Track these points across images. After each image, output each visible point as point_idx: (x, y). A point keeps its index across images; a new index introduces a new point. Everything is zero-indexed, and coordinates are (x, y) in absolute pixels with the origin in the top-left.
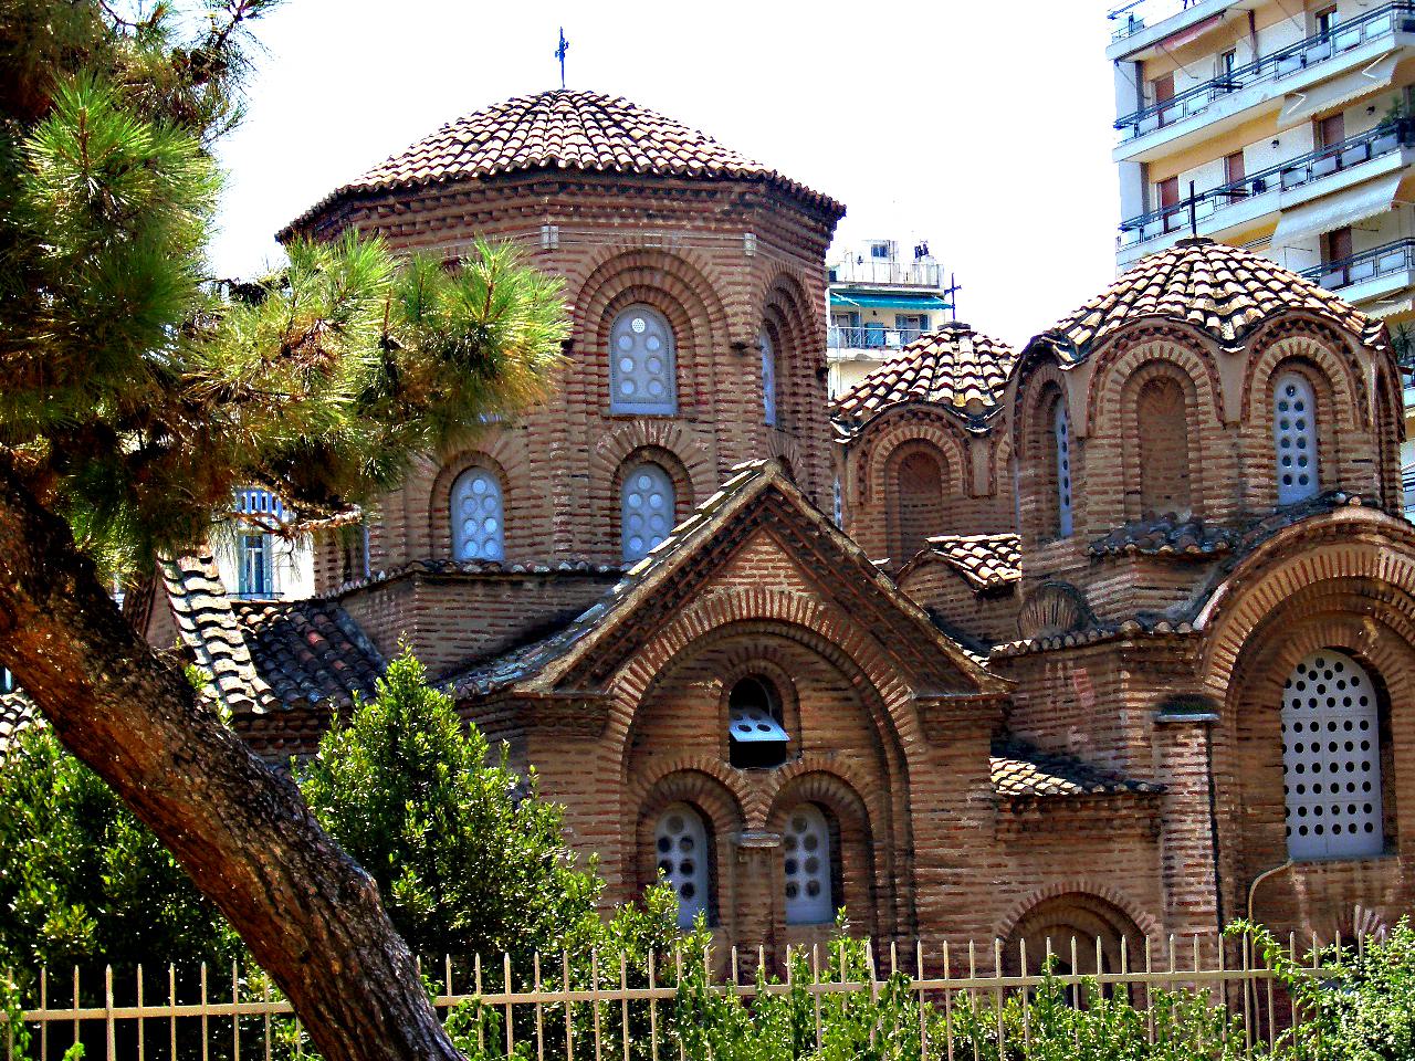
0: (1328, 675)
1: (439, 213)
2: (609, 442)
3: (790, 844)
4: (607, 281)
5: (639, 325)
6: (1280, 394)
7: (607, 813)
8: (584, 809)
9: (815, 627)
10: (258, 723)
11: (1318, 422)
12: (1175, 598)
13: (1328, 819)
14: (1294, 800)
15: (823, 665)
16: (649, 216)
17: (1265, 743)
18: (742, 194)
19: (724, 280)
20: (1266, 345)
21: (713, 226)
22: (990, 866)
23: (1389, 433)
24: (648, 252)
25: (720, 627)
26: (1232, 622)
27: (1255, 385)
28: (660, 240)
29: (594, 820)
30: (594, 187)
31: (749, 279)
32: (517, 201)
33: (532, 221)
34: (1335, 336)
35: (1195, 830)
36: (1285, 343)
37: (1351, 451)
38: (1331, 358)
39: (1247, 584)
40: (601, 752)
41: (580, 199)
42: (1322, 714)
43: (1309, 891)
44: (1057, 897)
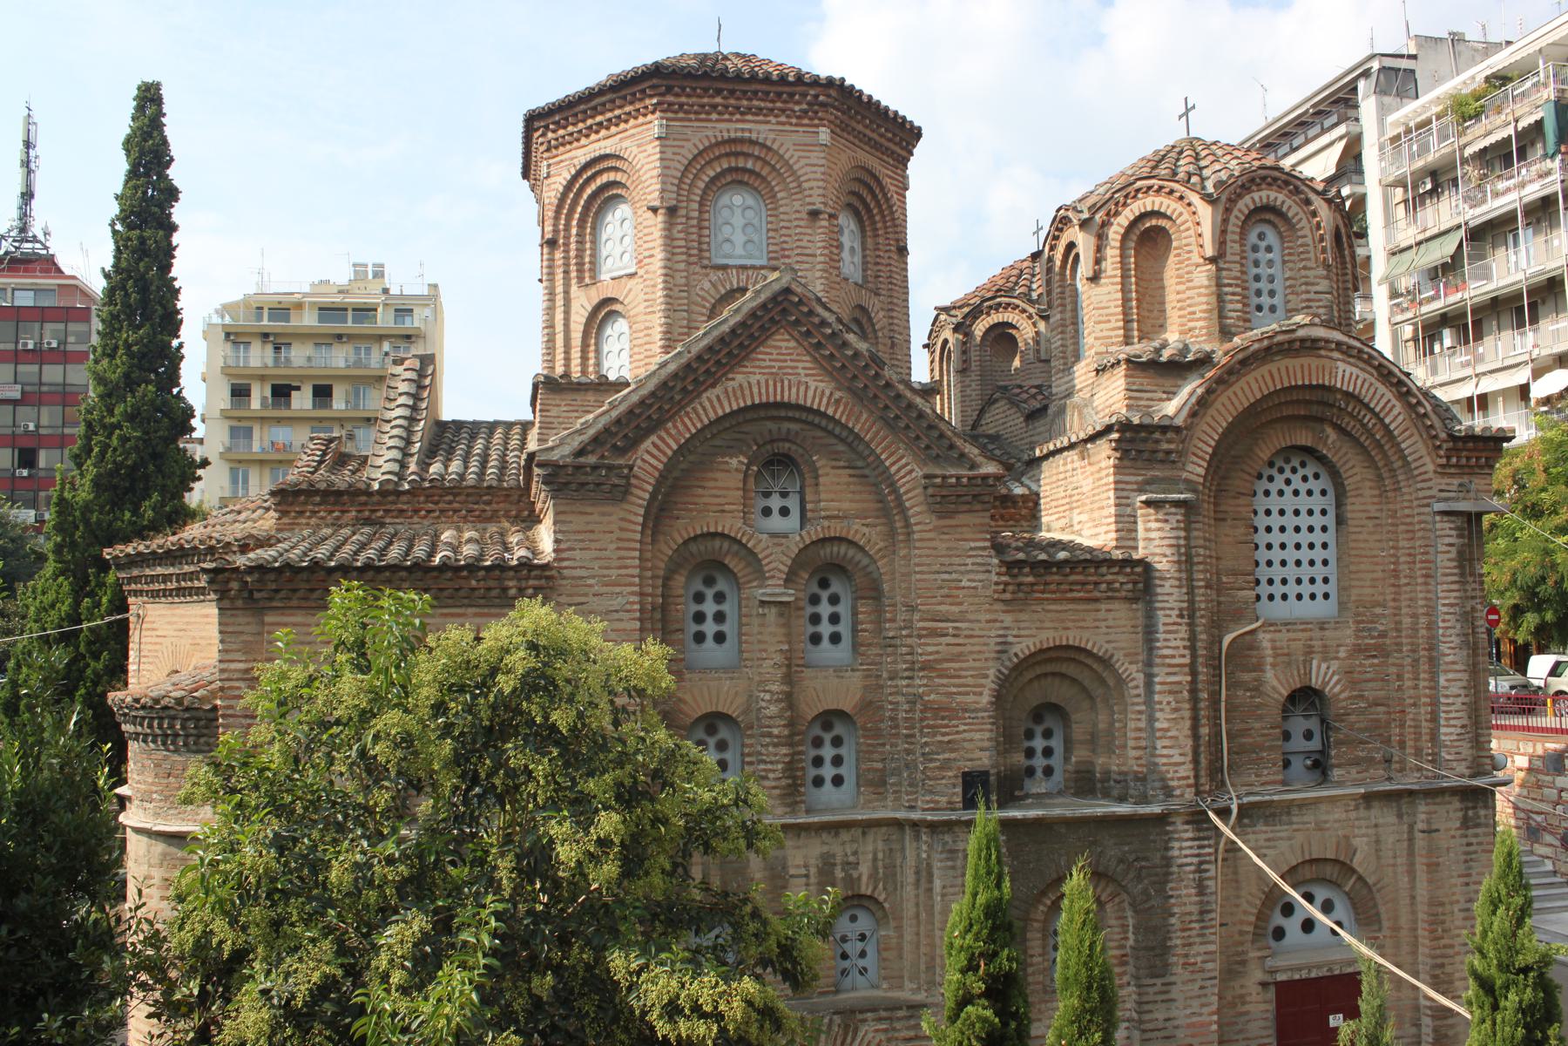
0: (1294, 471)
2: (707, 285)
3: (815, 600)
4: (707, 163)
5: (737, 200)
6: (1253, 237)
7: (626, 567)
8: (602, 563)
9: (830, 412)
10: (404, 498)
12: (1161, 400)
13: (1292, 589)
14: (1263, 573)
15: (841, 447)
16: (742, 114)
18: (816, 96)
19: (803, 162)
20: (1240, 196)
21: (794, 121)
22: (988, 621)
23: (1345, 282)
24: (741, 141)
25: (733, 413)
26: (1209, 419)
27: (1230, 228)
28: (750, 131)
29: (614, 572)
30: (694, 89)
31: (823, 162)
34: (1297, 191)
35: (1169, 596)
36: (1256, 196)
37: (1313, 284)
38: (1295, 209)
39: (1221, 388)
40: (622, 514)
41: (683, 99)
42: (1288, 502)
43: (1274, 648)
44: (1049, 649)
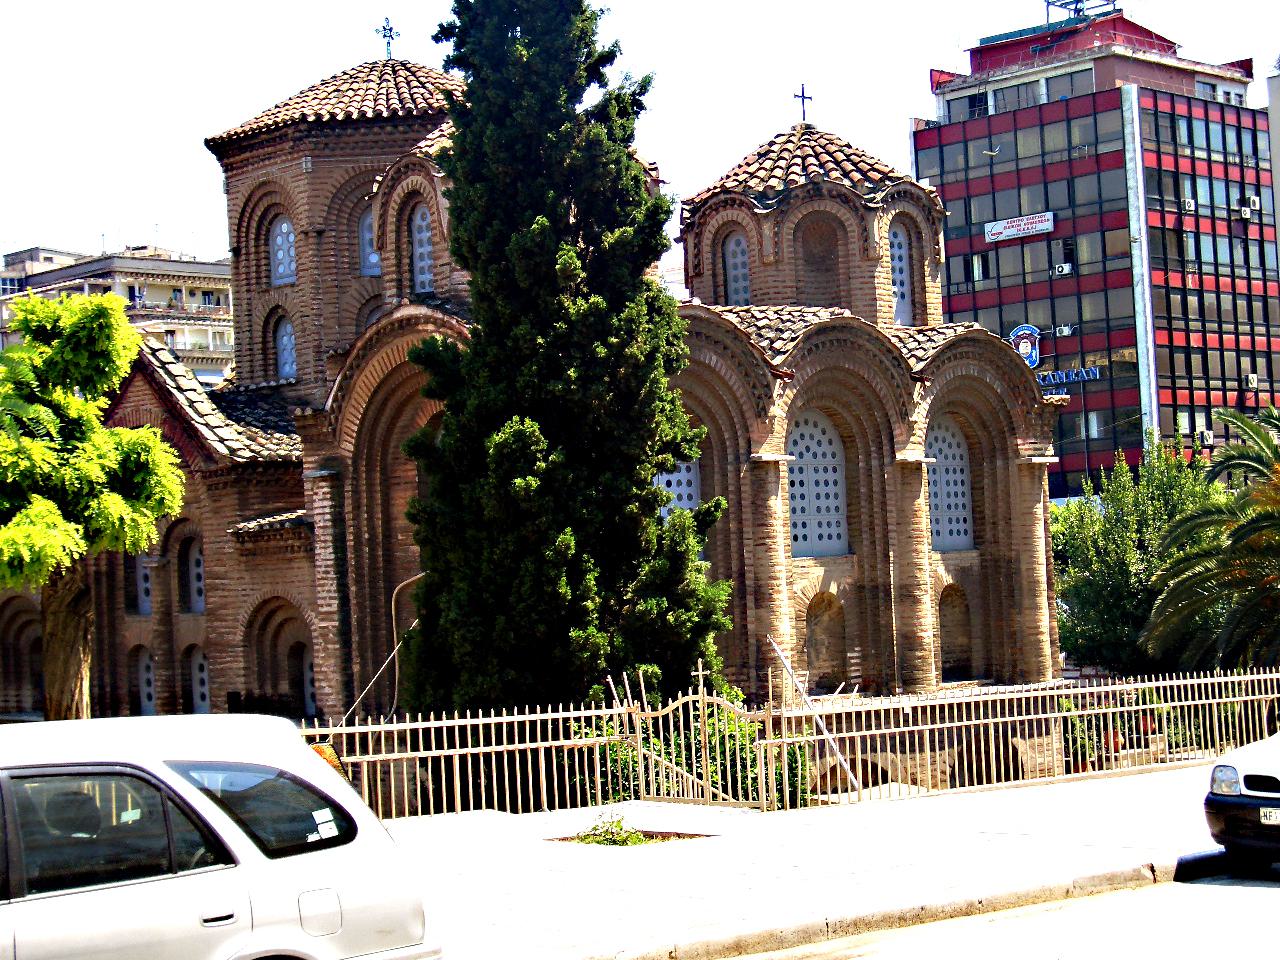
17: (409, 485)
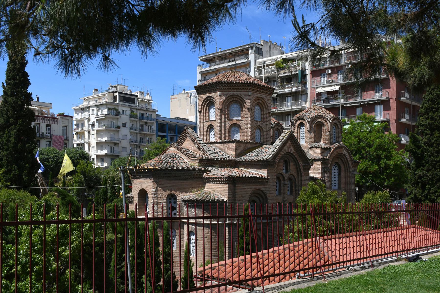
1: (233, 87)
11: (336, 132)
15: (292, 160)
32: (245, 87)
33: (248, 91)
34: (339, 121)
